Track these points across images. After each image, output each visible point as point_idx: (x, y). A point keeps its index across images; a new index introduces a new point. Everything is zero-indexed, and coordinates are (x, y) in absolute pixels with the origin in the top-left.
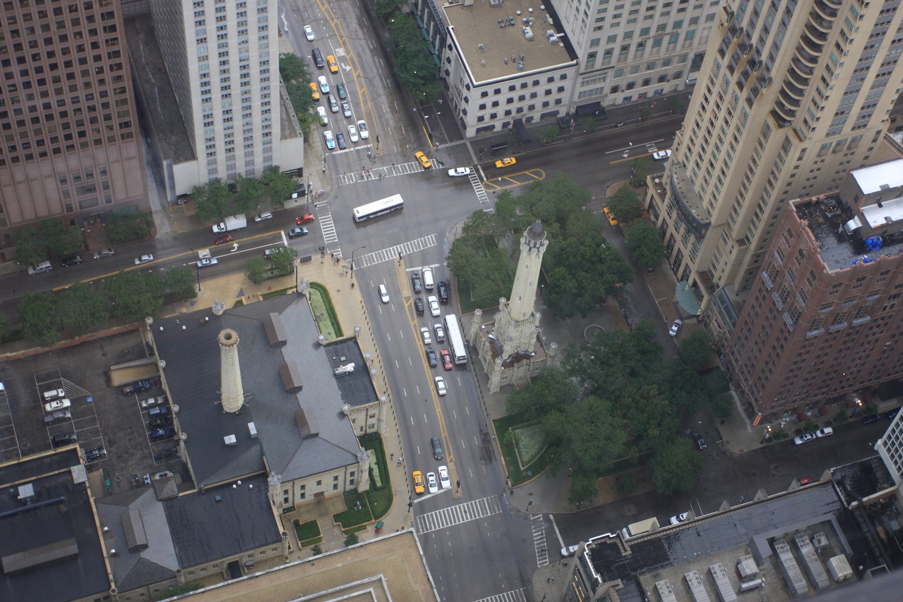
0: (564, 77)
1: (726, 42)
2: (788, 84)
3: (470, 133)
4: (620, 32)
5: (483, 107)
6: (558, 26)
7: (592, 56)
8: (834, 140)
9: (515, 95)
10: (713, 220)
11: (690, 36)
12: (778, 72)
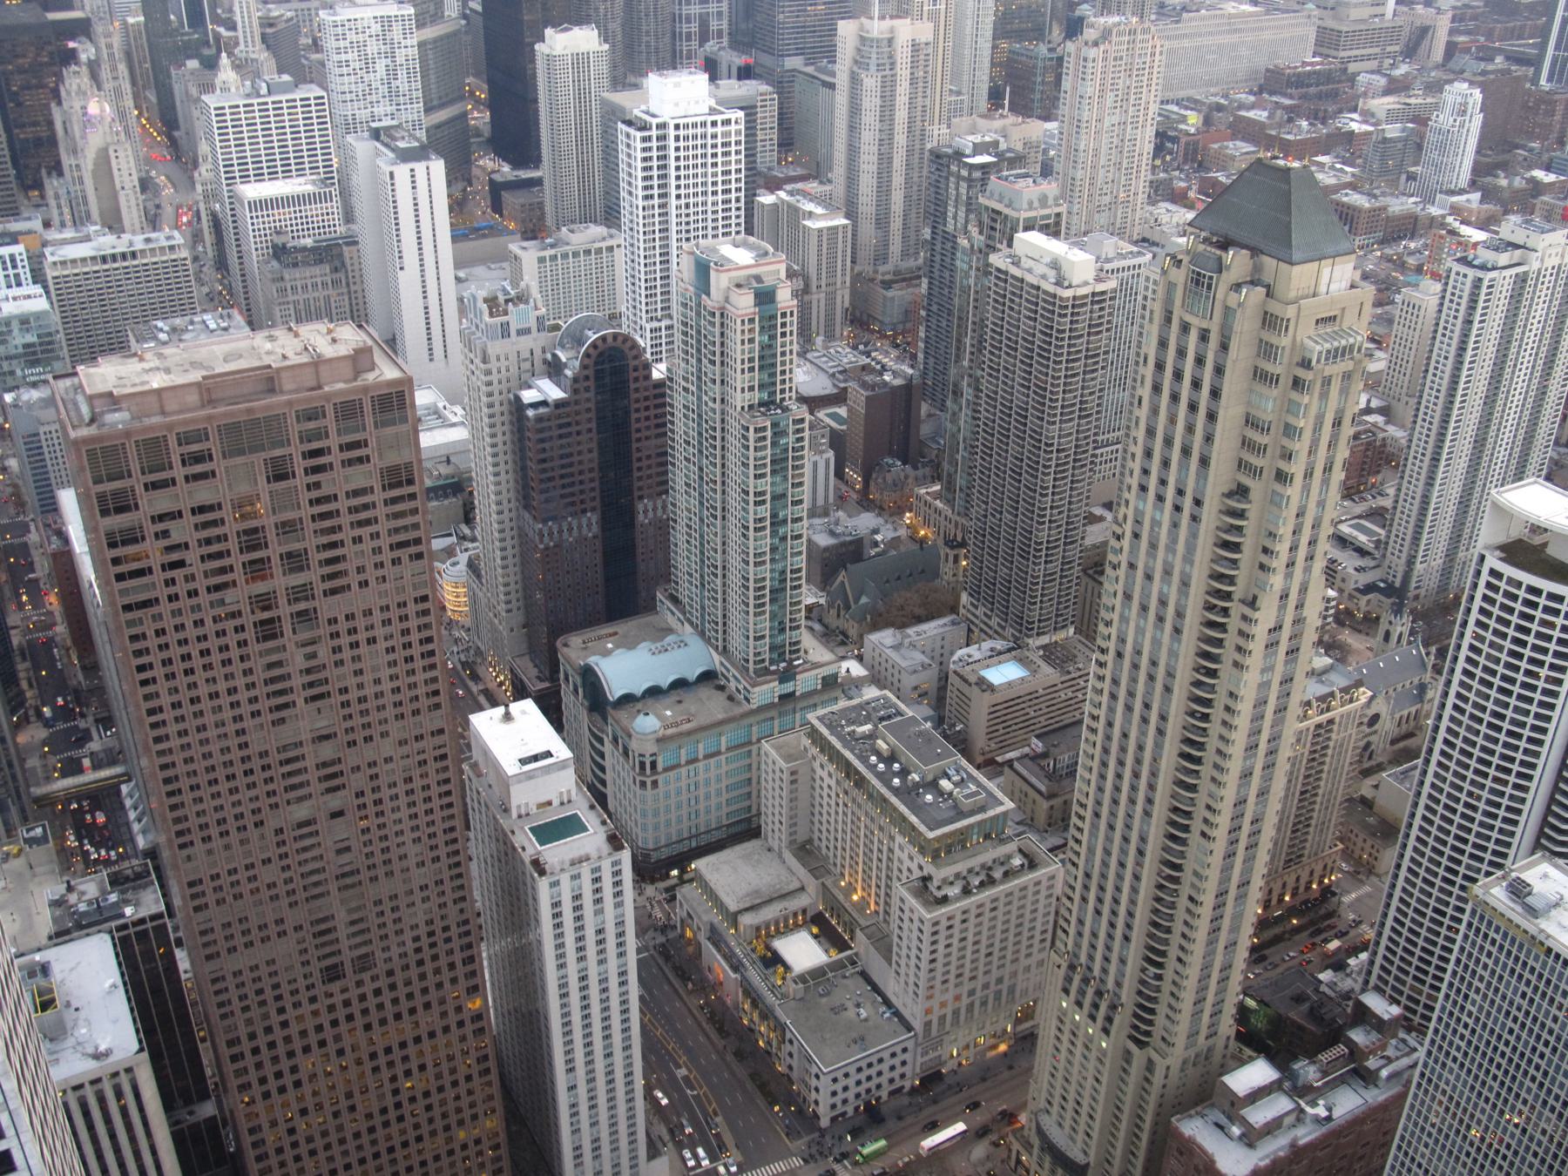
0: (905, 1050)
1: (1069, 979)
2: (1141, 1006)
3: (824, 1122)
4: (949, 996)
5: (834, 1094)
6: (887, 1002)
7: (928, 1024)
8: (1192, 1053)
9: (862, 1076)
10: (1092, 1159)
11: (1012, 990)
12: (1127, 996)
